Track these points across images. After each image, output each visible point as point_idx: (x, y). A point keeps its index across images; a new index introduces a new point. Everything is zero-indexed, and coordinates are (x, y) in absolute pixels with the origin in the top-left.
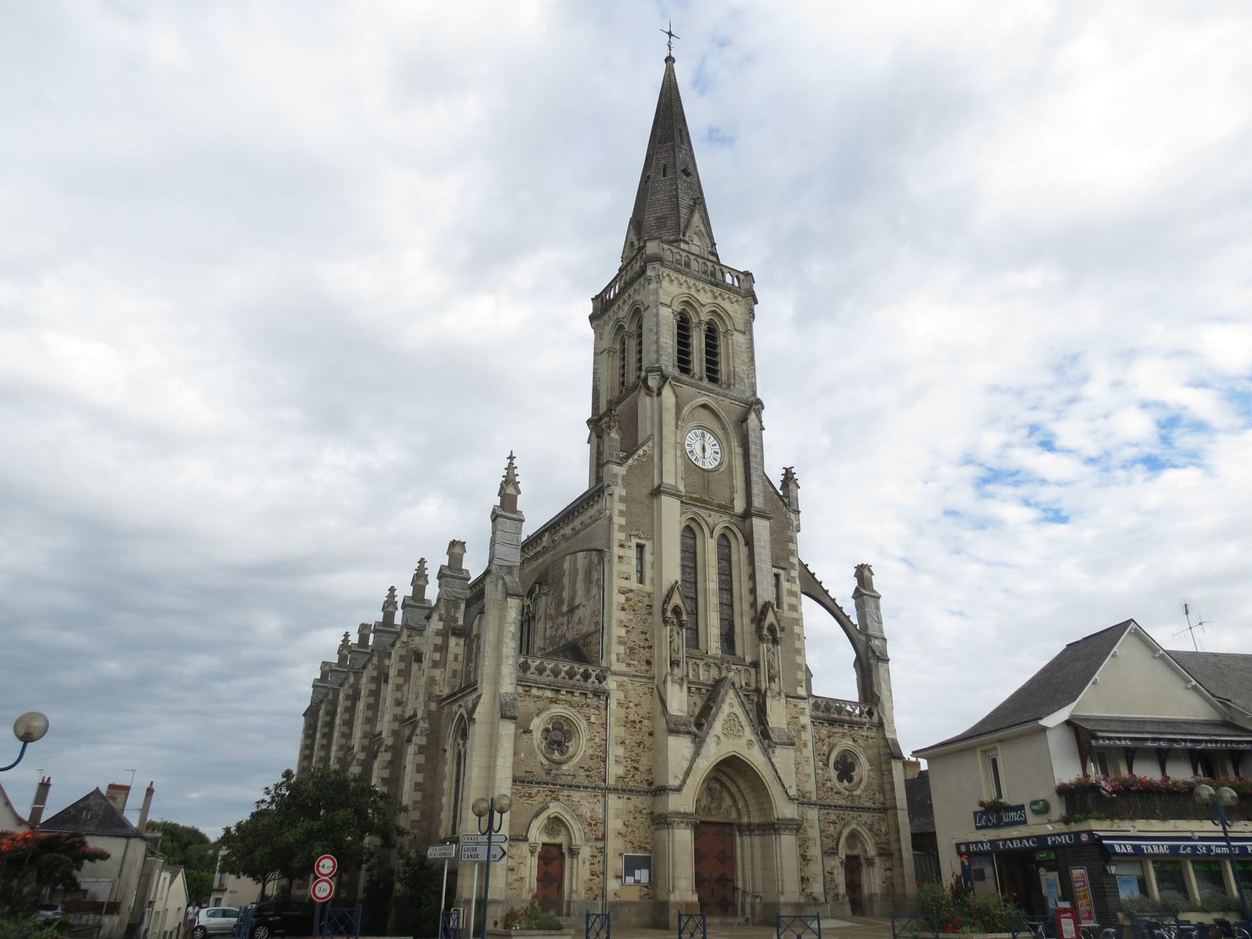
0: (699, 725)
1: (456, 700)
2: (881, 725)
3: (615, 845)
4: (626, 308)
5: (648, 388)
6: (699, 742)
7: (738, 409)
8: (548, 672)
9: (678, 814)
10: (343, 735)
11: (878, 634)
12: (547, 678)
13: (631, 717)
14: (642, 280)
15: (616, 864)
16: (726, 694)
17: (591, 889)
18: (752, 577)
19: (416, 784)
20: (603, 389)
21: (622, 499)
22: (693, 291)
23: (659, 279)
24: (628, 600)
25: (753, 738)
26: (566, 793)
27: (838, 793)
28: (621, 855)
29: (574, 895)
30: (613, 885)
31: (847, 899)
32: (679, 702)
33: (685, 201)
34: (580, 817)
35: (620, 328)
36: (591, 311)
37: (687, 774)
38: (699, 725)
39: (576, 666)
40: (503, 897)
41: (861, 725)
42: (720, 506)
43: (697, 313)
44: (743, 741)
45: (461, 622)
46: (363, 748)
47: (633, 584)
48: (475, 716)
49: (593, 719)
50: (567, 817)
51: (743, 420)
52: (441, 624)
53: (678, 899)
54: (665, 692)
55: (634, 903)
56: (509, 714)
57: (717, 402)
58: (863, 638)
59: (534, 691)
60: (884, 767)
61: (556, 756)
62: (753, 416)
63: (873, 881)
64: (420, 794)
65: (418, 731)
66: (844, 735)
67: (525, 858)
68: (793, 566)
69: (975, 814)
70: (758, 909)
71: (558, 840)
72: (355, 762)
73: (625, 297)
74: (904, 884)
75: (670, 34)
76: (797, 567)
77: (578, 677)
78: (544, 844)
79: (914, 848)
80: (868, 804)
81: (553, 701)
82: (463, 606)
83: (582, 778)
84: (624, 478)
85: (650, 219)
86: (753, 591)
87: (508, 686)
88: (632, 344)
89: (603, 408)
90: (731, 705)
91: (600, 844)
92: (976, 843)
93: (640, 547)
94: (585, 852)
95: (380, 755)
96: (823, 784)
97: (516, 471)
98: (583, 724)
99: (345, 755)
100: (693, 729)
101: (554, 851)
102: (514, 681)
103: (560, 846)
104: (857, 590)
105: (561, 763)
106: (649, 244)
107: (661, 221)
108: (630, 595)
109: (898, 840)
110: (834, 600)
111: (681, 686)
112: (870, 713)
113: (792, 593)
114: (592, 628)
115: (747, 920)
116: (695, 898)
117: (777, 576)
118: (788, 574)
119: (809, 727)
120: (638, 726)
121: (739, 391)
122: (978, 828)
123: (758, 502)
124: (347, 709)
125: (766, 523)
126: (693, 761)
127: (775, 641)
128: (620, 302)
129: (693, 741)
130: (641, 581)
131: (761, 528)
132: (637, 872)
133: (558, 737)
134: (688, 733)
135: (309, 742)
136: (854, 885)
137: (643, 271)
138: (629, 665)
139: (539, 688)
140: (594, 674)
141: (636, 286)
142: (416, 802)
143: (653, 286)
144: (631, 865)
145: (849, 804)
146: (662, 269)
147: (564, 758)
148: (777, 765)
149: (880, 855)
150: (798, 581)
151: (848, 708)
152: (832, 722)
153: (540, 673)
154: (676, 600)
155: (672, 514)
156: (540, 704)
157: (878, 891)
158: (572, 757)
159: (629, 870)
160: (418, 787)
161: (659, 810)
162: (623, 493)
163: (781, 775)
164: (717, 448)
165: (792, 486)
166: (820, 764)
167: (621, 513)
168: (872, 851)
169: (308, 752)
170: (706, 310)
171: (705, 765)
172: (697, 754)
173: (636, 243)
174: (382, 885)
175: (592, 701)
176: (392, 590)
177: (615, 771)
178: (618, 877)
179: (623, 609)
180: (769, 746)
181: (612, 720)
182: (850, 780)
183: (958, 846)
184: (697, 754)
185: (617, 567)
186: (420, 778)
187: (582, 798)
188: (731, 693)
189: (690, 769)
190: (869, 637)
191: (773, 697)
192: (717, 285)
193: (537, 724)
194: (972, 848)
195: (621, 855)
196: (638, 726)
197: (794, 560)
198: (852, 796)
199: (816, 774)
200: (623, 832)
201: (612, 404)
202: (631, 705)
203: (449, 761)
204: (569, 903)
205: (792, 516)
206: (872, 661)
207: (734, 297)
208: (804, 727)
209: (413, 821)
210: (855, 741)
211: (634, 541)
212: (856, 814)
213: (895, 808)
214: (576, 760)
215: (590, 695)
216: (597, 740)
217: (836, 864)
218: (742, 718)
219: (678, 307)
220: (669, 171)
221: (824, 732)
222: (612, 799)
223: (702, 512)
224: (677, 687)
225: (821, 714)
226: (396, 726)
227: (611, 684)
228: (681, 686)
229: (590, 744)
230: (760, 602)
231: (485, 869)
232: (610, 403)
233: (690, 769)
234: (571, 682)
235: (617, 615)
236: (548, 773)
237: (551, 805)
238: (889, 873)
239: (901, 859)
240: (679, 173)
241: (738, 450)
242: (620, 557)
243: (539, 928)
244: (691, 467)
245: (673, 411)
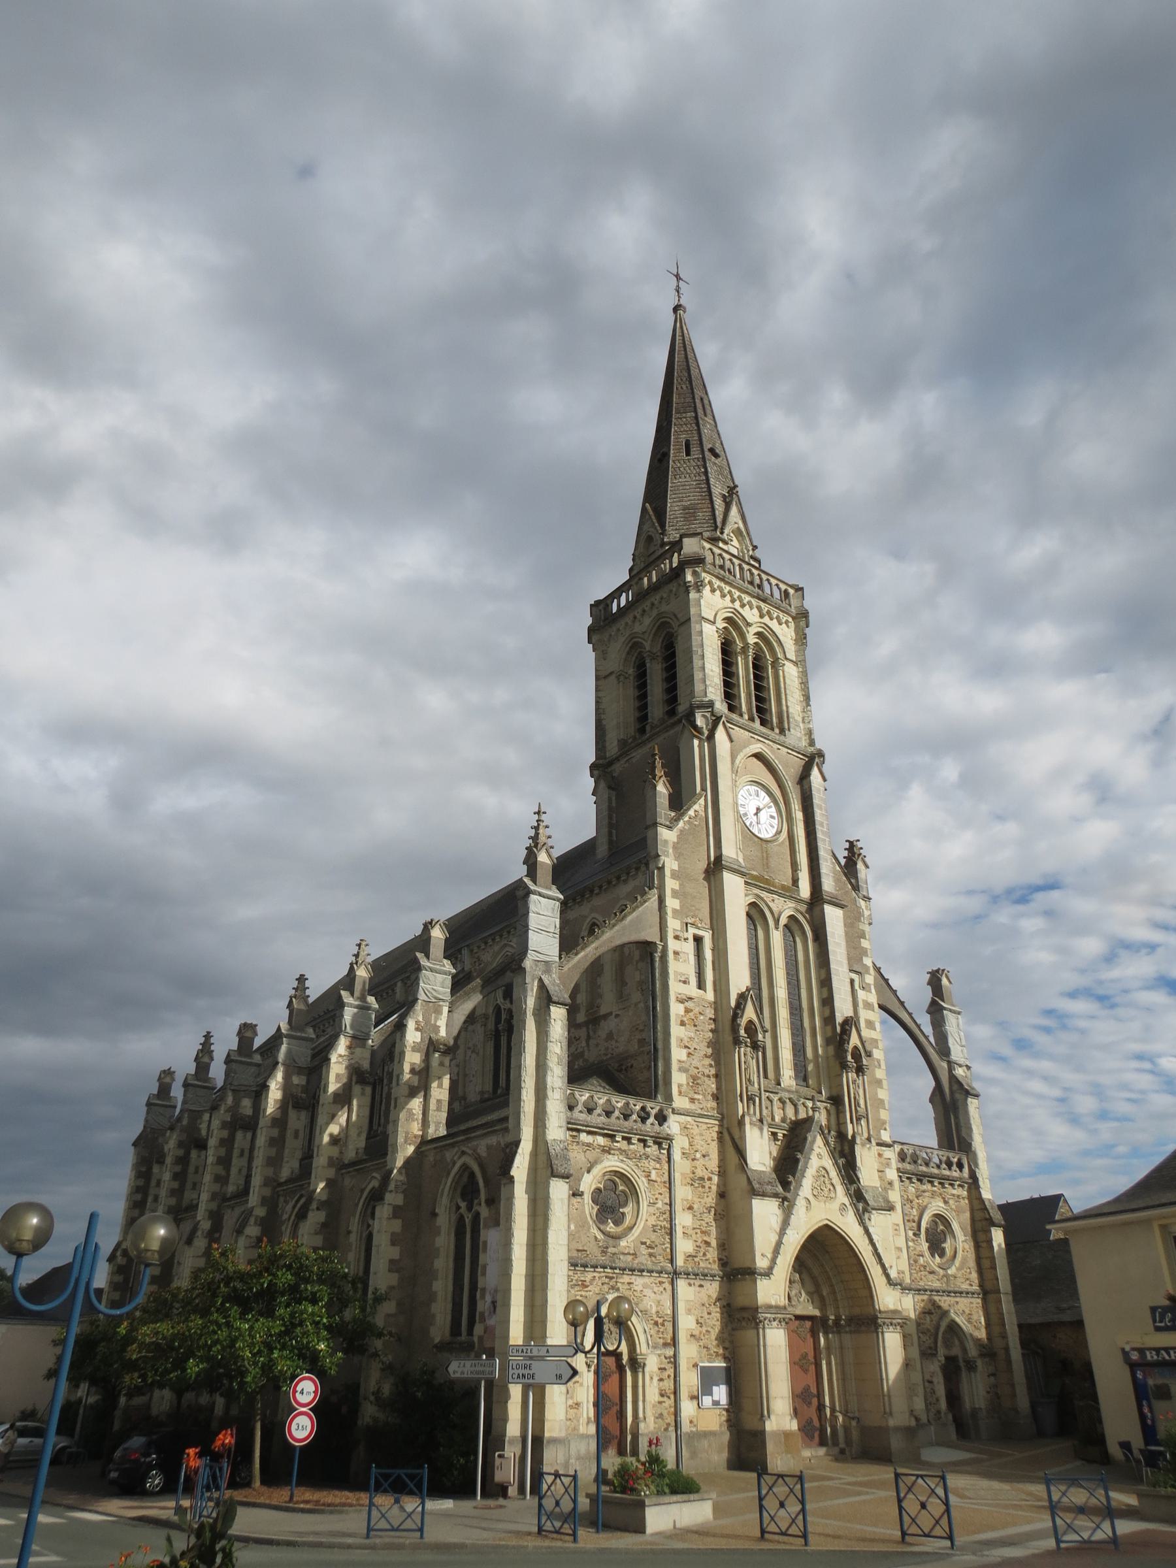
0: (785, 1185)
1: (453, 1145)
2: (973, 1183)
3: (688, 1351)
4: (647, 621)
5: (695, 727)
6: (787, 1205)
7: (797, 763)
8: (599, 1111)
9: (769, 1307)
10: (218, 1179)
11: (962, 1061)
12: (597, 1119)
13: (700, 1172)
14: (673, 586)
15: (690, 1380)
16: (814, 1141)
17: (661, 1416)
18: (826, 982)
19: (391, 1261)
20: (610, 724)
21: (675, 875)
22: (737, 604)
23: (699, 586)
24: (687, 1011)
25: (846, 1201)
26: (626, 1279)
27: (932, 1272)
28: (695, 1365)
29: (642, 1425)
30: (688, 1408)
31: (950, 1417)
32: (760, 1152)
33: (718, 490)
35: (634, 646)
36: (589, 621)
37: (776, 1251)
38: (785, 1185)
39: (632, 1102)
40: (563, 1434)
41: (951, 1181)
42: (783, 887)
43: (743, 636)
44: (836, 1205)
45: (443, 1033)
46: (264, 1201)
47: (692, 990)
48: (514, 1172)
49: (653, 1176)
51: (804, 778)
52: (418, 1034)
53: (775, 1428)
54: (743, 1137)
55: (712, 1434)
56: (561, 1170)
57: (772, 751)
58: (945, 1065)
59: (584, 1137)
60: (981, 1237)
61: (610, 1227)
62: (815, 773)
63: (976, 1391)
64: (395, 1276)
65: (392, 1186)
66: (933, 1194)
68: (867, 968)
69: (1153, 1310)
70: (855, 1435)
72: (252, 1220)
73: (646, 605)
74: (1014, 1395)
75: (677, 276)
76: (872, 971)
77: (634, 1117)
79: (1022, 1348)
80: (965, 1287)
81: (607, 1151)
82: (445, 1010)
83: (644, 1260)
84: (675, 848)
85: (673, 507)
86: (828, 1001)
87: (556, 1131)
88: (655, 671)
89: (613, 749)
90: (819, 1155)
91: (670, 1352)
92: (1157, 1350)
93: (698, 940)
94: (652, 1363)
95: (310, 1214)
96: (916, 1261)
97: (548, 832)
98: (642, 1184)
99: (219, 1207)
100: (780, 1189)
101: (611, 1361)
102: (564, 1124)
104: (933, 1003)
105: (617, 1238)
106: (686, 541)
107: (690, 513)
108: (690, 1004)
109: (1004, 1336)
110: (910, 1014)
111: (761, 1130)
112: (960, 1166)
113: (868, 1006)
114: (634, 1047)
115: (842, 1452)
116: (794, 1426)
117: (852, 981)
118: (862, 980)
119: (897, 1184)
120: (707, 1184)
121: (797, 736)
122: (1158, 1329)
123: (828, 885)
124: (223, 1142)
125: (839, 912)
126: (782, 1233)
127: (860, 1070)
128: (637, 612)
129: (781, 1205)
130: (701, 985)
131: (833, 917)
132: (715, 1389)
133: (613, 1201)
134: (776, 1195)
135: (141, 1182)
136: (953, 1398)
137: (678, 573)
138: (692, 1100)
139: (589, 1133)
140: (653, 1112)
141: (664, 593)
142: (391, 1288)
143: (693, 595)
144: (707, 1379)
145: (944, 1287)
146: (704, 575)
147: (620, 1229)
148: (875, 1237)
149: (982, 1355)
150: (873, 991)
151: (925, 1156)
152: (921, 1178)
153: (590, 1111)
154: (750, 1013)
155: (736, 894)
156: (591, 1155)
157: (983, 1406)
158: (631, 1228)
159: (706, 1389)
160: (394, 1265)
161: (741, 1301)
162: (676, 867)
163: (880, 1250)
164: (773, 811)
165: (860, 865)
166: (910, 1233)
167: (675, 894)
168: (973, 1352)
169: (139, 1197)
170: (753, 630)
171: (795, 1239)
172: (785, 1223)
173: (657, 537)
174: (344, 1409)
175: (653, 1150)
176: (302, 979)
177: (684, 1246)
178: (693, 1398)
179: (683, 1024)
180: (865, 1210)
181: (677, 1176)
182: (942, 1255)
183: (1125, 1354)
184: (785, 1223)
185: (673, 966)
186: (395, 1253)
187: (645, 1286)
188: (819, 1141)
189: (779, 1244)
190: (951, 1065)
191: (863, 1145)
192: (764, 601)
193: (589, 1183)
194: (1150, 1356)
195: (695, 1365)
196: (707, 1184)
197: (868, 961)
198: (946, 1276)
199: (908, 1247)
200: (696, 1333)
201: (626, 747)
202: (698, 1155)
203: (444, 1230)
205: (863, 903)
206: (958, 1096)
207: (784, 618)
208: (891, 1183)
209: (388, 1315)
210: (946, 1202)
211: (692, 931)
212: (953, 1300)
213: (998, 1291)
214: (636, 1232)
215: (650, 1142)
216: (660, 1205)
217: (935, 1368)
218: (833, 1173)
219: (721, 625)
220: (695, 450)
221: (911, 1189)
222: (681, 1284)
223: (764, 895)
224: (756, 1131)
225: (908, 1167)
226: (331, 1173)
227: (673, 1126)
228: (761, 1130)
229: (652, 1209)
230: (839, 1019)
231: (536, 1393)
232: (623, 743)
233: (779, 1244)
234: (626, 1124)
235: (676, 1031)
236: (604, 1252)
238: (992, 1378)
239: (1009, 1361)
240: (707, 454)
241: (799, 816)
242: (676, 953)
243: (674, 1492)
244: (748, 835)
245: (729, 759)
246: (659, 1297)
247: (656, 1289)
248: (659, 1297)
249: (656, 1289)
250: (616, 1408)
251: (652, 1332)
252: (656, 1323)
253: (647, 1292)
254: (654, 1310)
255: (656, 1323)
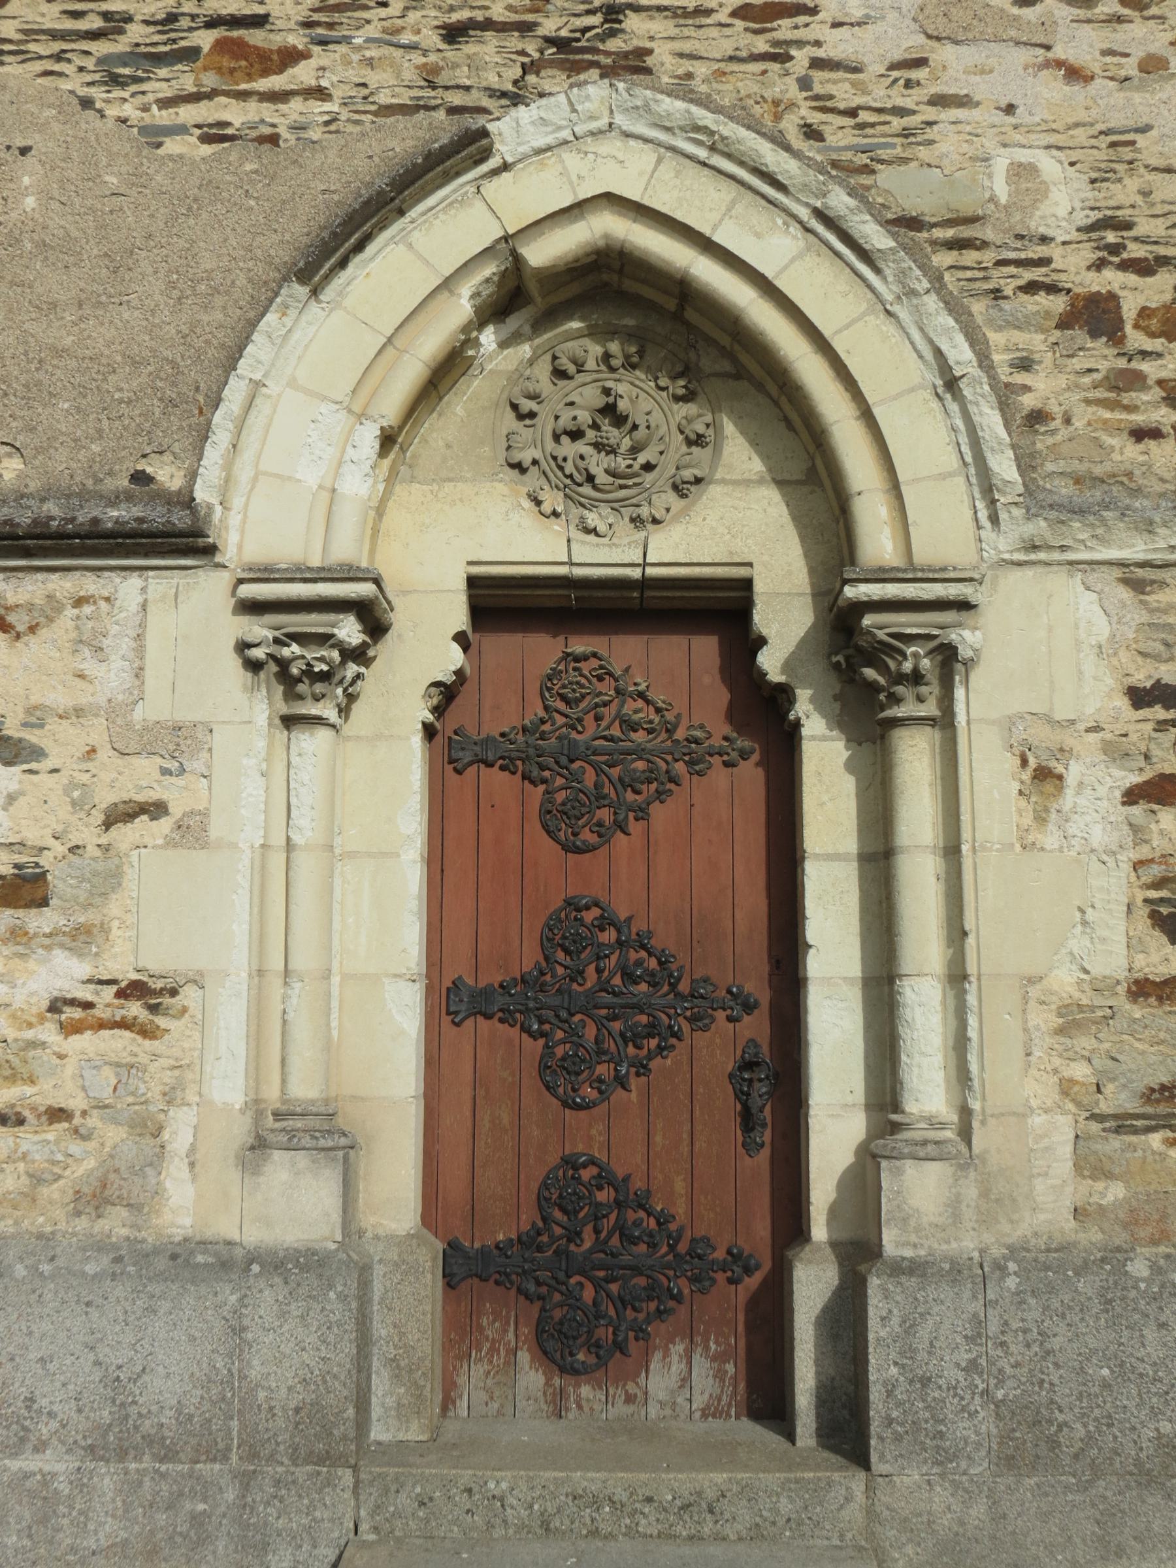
34: (944, 240)
50: (763, 255)
67: (177, 743)
71: (685, 543)
78: (500, 604)
103: (719, 608)
204: (859, 1254)
237: (512, 131)
246: (1109, 104)
247: (1081, 44)
248: (1109, 104)
249: (1081, 44)
250: (716, 1048)
251: (1043, 388)
252: (1096, 316)
253: (954, 66)
254: (1063, 204)
255: (1096, 316)
